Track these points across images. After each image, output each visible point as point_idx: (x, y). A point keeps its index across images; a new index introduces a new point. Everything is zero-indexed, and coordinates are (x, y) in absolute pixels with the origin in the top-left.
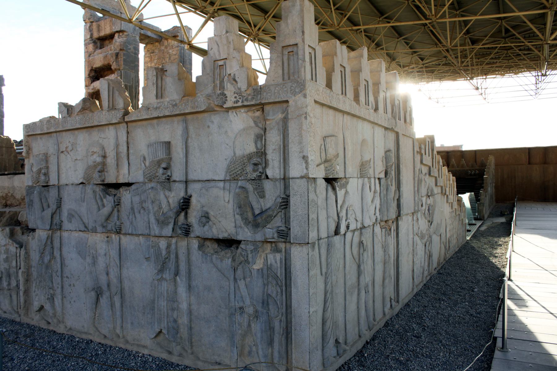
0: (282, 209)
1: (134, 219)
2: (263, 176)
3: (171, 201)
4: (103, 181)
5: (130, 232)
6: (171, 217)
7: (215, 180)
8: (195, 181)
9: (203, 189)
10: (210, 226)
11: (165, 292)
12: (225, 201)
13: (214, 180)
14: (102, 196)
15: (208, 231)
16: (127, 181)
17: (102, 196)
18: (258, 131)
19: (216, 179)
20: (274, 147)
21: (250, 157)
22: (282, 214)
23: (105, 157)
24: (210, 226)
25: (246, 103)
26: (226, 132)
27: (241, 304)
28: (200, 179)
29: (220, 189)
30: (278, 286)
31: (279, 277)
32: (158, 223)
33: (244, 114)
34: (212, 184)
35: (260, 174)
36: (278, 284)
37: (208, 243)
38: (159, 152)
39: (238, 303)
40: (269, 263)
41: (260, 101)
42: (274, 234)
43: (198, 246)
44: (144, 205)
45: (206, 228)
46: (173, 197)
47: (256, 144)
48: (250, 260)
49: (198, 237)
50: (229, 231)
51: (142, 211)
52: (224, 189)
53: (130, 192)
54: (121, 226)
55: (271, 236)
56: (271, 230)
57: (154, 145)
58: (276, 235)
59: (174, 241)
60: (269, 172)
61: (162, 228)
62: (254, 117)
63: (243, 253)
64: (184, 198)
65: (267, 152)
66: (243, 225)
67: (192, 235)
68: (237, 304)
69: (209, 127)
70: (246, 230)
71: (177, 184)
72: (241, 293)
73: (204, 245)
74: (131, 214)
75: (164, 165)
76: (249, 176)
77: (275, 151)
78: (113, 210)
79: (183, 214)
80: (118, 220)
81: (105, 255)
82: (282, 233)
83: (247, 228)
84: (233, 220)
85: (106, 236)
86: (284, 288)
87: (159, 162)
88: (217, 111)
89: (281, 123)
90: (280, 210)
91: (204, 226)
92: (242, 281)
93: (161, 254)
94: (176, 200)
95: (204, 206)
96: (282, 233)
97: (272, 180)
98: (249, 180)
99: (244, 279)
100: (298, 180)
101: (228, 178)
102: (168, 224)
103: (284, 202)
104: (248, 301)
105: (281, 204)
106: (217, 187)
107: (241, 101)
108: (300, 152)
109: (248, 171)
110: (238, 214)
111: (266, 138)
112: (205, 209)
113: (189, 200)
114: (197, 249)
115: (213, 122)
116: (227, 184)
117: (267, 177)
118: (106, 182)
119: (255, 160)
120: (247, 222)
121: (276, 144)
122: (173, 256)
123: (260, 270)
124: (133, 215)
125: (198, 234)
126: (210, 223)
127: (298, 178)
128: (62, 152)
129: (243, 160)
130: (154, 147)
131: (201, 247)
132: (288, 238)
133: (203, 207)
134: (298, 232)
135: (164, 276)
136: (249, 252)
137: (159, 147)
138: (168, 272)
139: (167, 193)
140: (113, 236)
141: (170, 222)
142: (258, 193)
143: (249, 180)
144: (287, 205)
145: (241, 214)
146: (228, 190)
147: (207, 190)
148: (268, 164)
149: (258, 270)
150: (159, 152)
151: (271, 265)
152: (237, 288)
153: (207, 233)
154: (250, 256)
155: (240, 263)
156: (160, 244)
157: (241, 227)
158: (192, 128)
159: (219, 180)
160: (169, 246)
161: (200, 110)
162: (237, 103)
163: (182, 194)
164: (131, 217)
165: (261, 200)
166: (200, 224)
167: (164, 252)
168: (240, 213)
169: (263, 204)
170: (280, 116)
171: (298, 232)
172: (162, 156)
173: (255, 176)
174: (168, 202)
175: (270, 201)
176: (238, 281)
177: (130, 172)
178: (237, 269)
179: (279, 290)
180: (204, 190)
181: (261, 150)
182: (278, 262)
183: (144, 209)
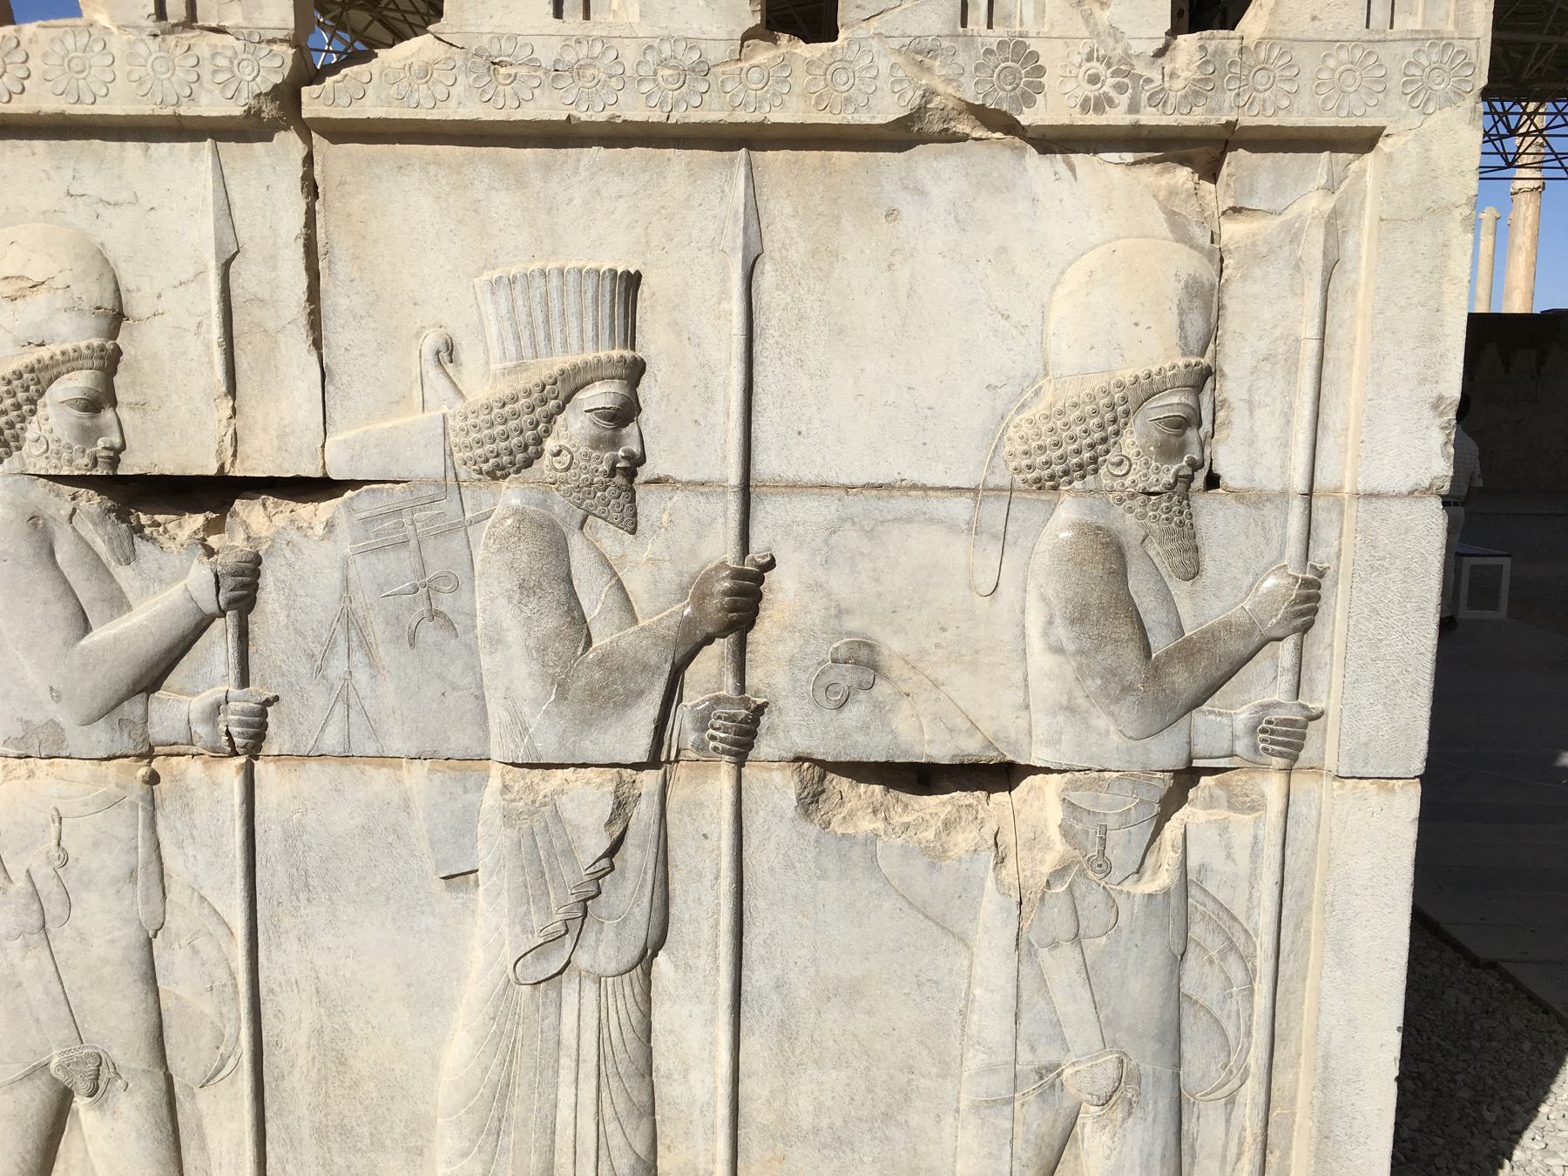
0: (1295, 630)
1: (362, 677)
2: (1200, 477)
3: (636, 584)
4: (114, 461)
5: (332, 741)
6: (645, 667)
7: (925, 488)
8: (795, 487)
9: (848, 525)
10: (877, 706)
11: (589, 1038)
12: (971, 587)
13: (914, 487)
14: (101, 547)
15: (865, 728)
16: (311, 470)
17: (101, 547)
18: (1189, 263)
19: (929, 481)
20: (1263, 346)
21: (1148, 390)
22: (1286, 650)
23: (116, 318)
24: (877, 706)
25: (1150, 117)
26: (1003, 250)
27: (1048, 1055)
28: (831, 477)
29: (951, 527)
30: (1232, 959)
31: (1242, 918)
32: (562, 695)
33: (1118, 172)
34: (902, 504)
35: (1188, 471)
36: (1232, 946)
37: (840, 784)
38: (573, 323)
39: (1033, 1049)
40: (1193, 863)
41: (1232, 118)
42: (1234, 737)
43: (799, 799)
44: (445, 603)
45: (856, 712)
46: (652, 561)
47: (1182, 326)
48: (1114, 853)
49: (798, 759)
50: (988, 727)
51: (430, 634)
52: (975, 529)
53: (330, 526)
54: (264, 714)
55: (1225, 746)
56: (1225, 720)
57: (539, 282)
58: (1241, 746)
59: (649, 780)
60: (1228, 463)
61: (586, 723)
62: (1173, 192)
63: (1079, 827)
64: (738, 575)
65: (1226, 369)
66: (1081, 701)
67: (764, 747)
68: (1025, 1056)
69: (891, 214)
70: (1101, 721)
71: (678, 497)
72: (1050, 1002)
73: (823, 791)
74: (342, 648)
75: (601, 395)
76: (1130, 477)
77: (1268, 367)
78: (202, 625)
79: (721, 647)
80: (244, 681)
81: (132, 874)
82: (1286, 734)
83: (1112, 714)
84: (1018, 676)
85: (143, 771)
86: (1264, 966)
87: (570, 384)
88: (964, 138)
89: (1318, 235)
90: (1279, 633)
91: (841, 706)
92: (1068, 951)
93: (569, 853)
94: (669, 576)
95: (847, 612)
96: (1286, 734)
97: (1239, 495)
98: (1133, 496)
99: (1076, 938)
100: (1397, 505)
101: (1001, 478)
102: (635, 696)
103: (1308, 598)
104: (1082, 1034)
105: (1297, 608)
106: (931, 520)
107: (1123, 100)
108: (1423, 381)
109: (1130, 452)
110: (1058, 650)
111: (1226, 301)
112: (853, 624)
113: (759, 579)
114: (790, 813)
115: (920, 192)
116: (994, 511)
117: (1213, 481)
118: (130, 466)
119: (1174, 402)
120: (1115, 689)
121: (1278, 332)
122: (636, 855)
123: (1160, 897)
124: (358, 656)
125: (803, 745)
126: (882, 689)
127: (1398, 496)
129: (1112, 406)
130: (536, 296)
131: (811, 800)
132: (1303, 754)
133: (840, 613)
134: (1378, 728)
135: (583, 960)
136: (1112, 822)
137: (572, 298)
138: (609, 934)
139: (609, 538)
140: (193, 769)
141: (641, 693)
142: (1169, 554)
143: (1133, 496)
144: (1315, 611)
145: (1081, 652)
146: (994, 536)
147: (870, 533)
148: (1228, 423)
149: (1150, 895)
150: (573, 323)
151: (1203, 868)
152: (1028, 984)
153: (860, 738)
154: (1114, 837)
155: (1060, 872)
156: (563, 801)
157: (1071, 710)
158: (788, 210)
159: (943, 489)
160: (621, 806)
161: (864, 118)
163: (720, 547)
164: (337, 667)
165: (1179, 589)
166: (821, 693)
167: (597, 844)
168: (1071, 648)
169: (1184, 607)
170: (1314, 203)
171: (1378, 728)
172: (589, 345)
173: (1168, 478)
174: (620, 586)
175: (1228, 589)
176: (1044, 952)
177: (335, 414)
178: (1042, 899)
179: (1237, 974)
180: (851, 537)
181: (1202, 354)
183: (450, 624)
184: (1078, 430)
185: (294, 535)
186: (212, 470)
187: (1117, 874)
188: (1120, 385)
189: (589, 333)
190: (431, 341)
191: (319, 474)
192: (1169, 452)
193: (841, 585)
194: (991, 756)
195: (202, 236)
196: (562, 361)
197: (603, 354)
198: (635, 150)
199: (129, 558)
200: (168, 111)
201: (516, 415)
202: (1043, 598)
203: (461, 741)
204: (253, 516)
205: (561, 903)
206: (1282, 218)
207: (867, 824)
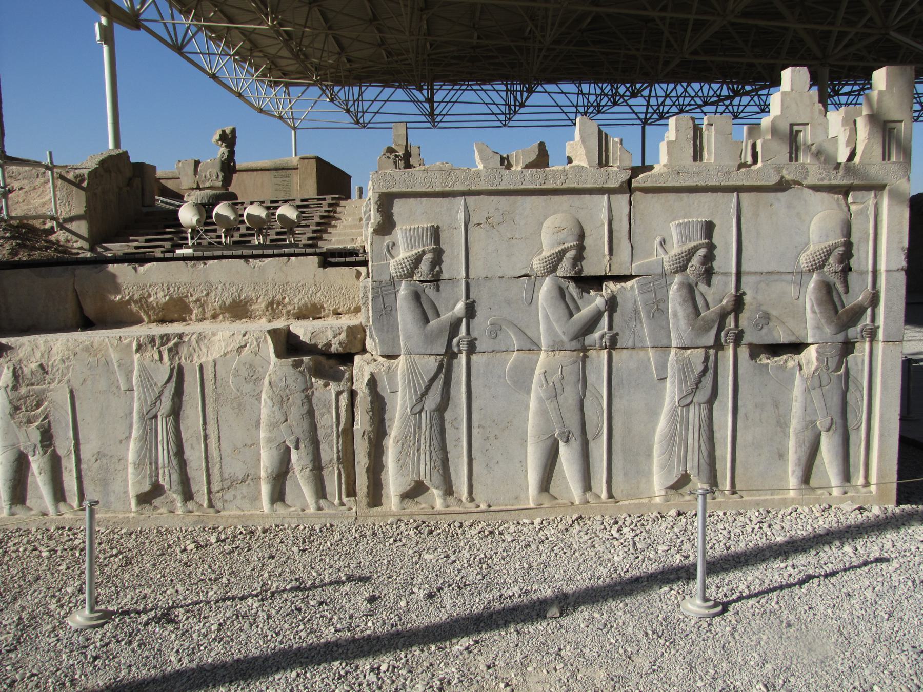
3: (709, 300)
5: (630, 344)
19: (782, 270)
34: (776, 277)
45: (765, 330)
55: (855, 336)
59: (712, 352)
75: (702, 252)
106: (783, 281)
112: (763, 308)
128: (479, 224)
133: (760, 305)
135: (695, 400)
147: (767, 285)
155: (816, 370)
162: (822, 180)
180: (762, 285)
182: (860, 364)
184: (819, 257)
185: (623, 290)
186: (603, 274)
187: (830, 370)
188: (829, 246)
189: (699, 237)
190: (658, 240)
191: (629, 274)
192: (841, 262)
193: (760, 297)
194: (798, 341)
195: (604, 215)
196: (692, 244)
197: (704, 241)
198: (719, 193)
199: (581, 297)
200: (600, 186)
201: (683, 257)
202: (811, 299)
203: (664, 342)
204: (610, 288)
205: (690, 383)
206: (862, 205)
207: (765, 361)
